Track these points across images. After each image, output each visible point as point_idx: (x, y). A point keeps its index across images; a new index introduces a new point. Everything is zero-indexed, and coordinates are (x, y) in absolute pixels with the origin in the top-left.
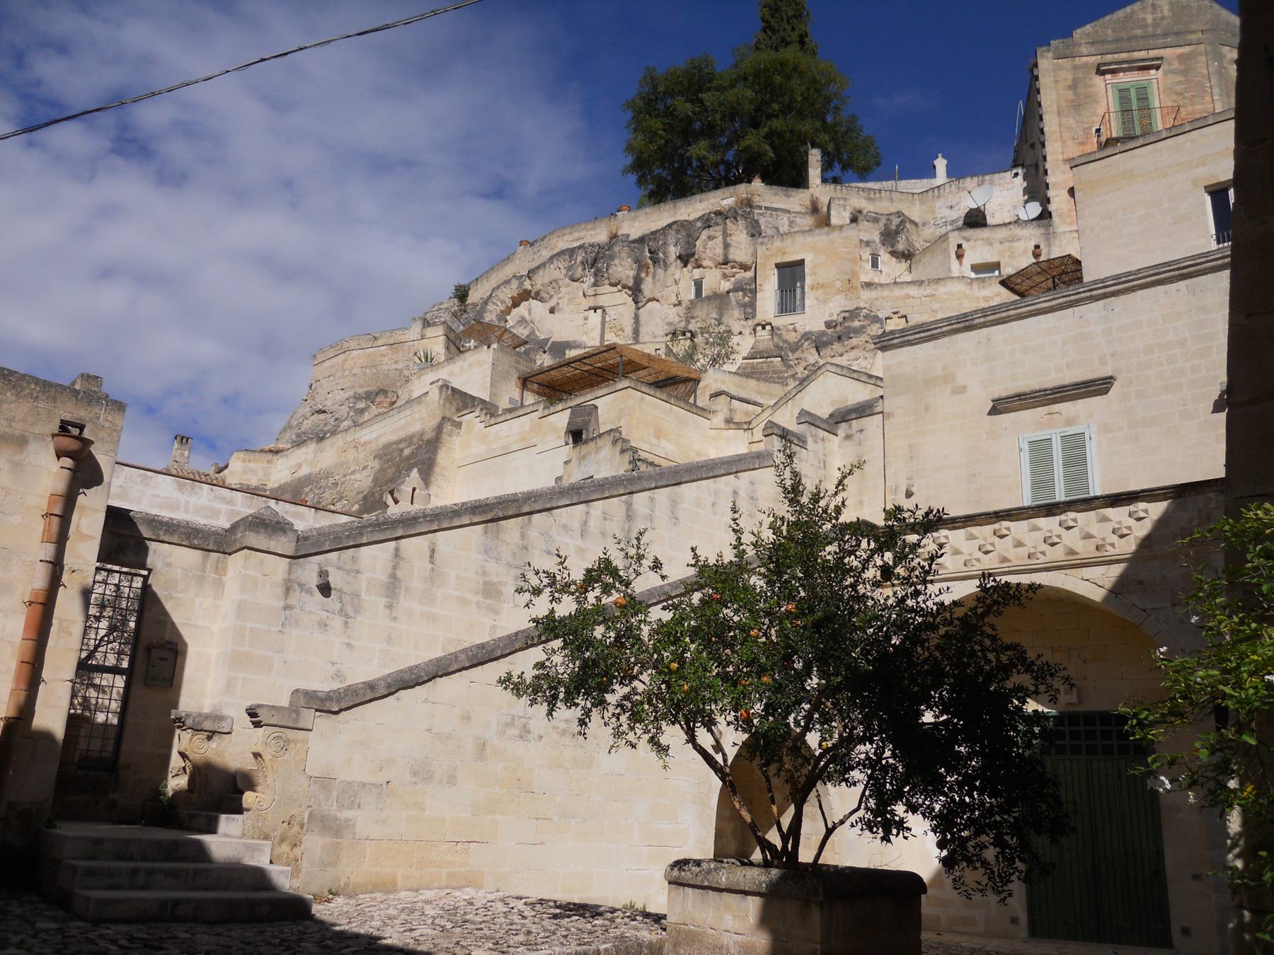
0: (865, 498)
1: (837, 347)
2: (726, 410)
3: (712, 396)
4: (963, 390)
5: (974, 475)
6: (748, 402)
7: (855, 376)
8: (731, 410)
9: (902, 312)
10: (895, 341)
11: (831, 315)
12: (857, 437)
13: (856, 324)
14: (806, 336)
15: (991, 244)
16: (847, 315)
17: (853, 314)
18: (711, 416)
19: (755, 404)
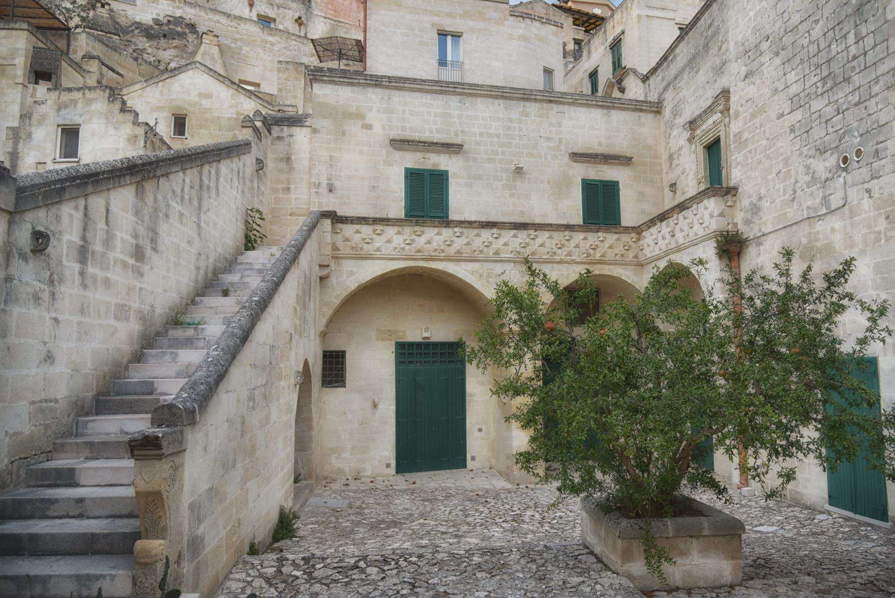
0: (292, 186)
1: (162, 41)
2: (98, 73)
3: (84, 57)
4: (369, 127)
5: (374, 187)
6: (113, 70)
7: (221, 78)
8: (101, 74)
9: (215, 33)
10: (325, 78)
11: (158, 14)
12: (287, 140)
13: (179, 29)
14: (138, 25)
15: (272, 4)
16: (171, 19)
17: (178, 21)
18: (85, 75)
19: (118, 73)
